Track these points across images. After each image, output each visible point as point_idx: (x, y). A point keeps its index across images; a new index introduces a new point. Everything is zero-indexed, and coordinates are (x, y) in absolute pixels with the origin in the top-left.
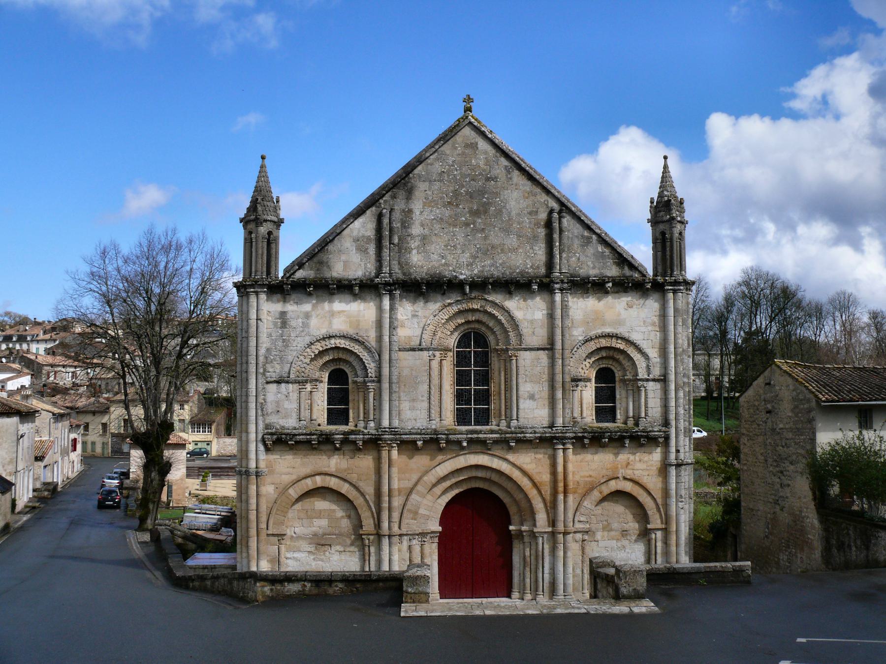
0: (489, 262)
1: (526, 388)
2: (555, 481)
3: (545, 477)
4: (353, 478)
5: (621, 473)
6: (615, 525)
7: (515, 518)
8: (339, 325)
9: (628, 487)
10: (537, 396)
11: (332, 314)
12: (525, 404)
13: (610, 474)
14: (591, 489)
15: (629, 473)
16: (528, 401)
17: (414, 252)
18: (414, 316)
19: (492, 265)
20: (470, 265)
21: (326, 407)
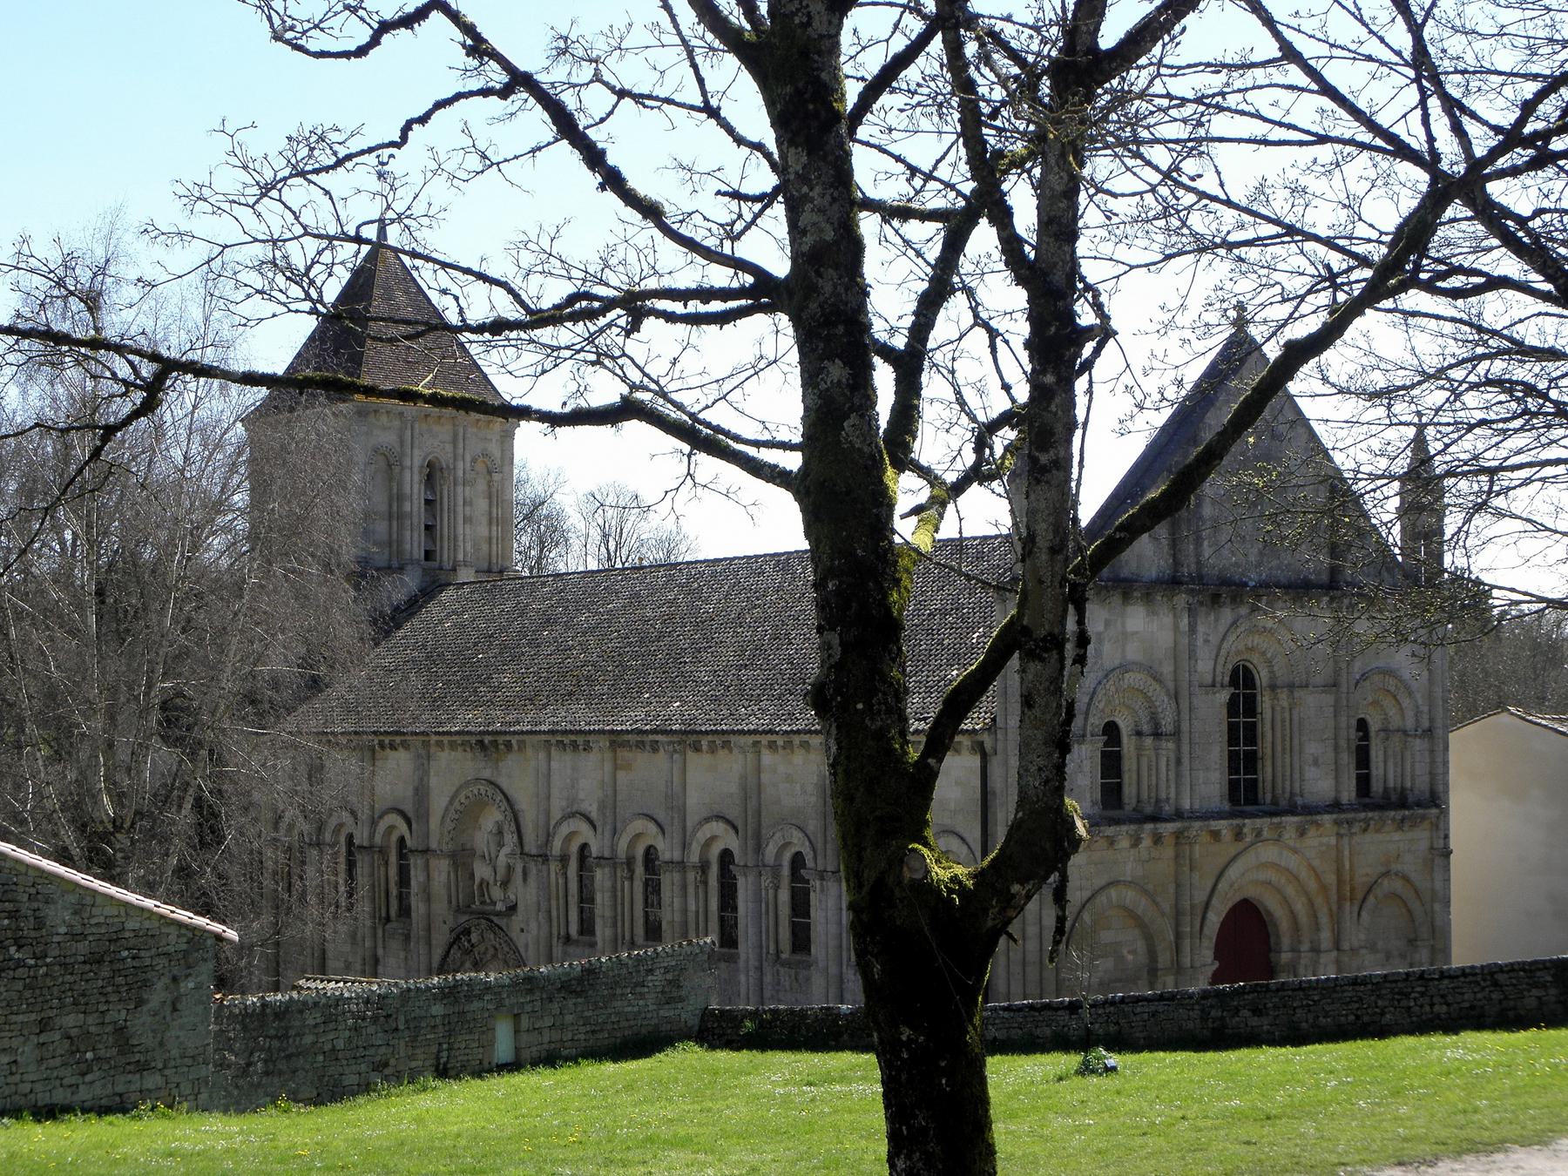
0: (1275, 563)
1: (1312, 748)
2: (1340, 882)
3: (1331, 879)
4: (1150, 887)
5: (1395, 867)
6: (1380, 944)
7: (1286, 942)
8: (1133, 652)
9: (1397, 885)
10: (1320, 761)
11: (1125, 636)
12: (1311, 773)
13: (1383, 870)
14: (1368, 892)
15: (1399, 867)
16: (1313, 769)
17: (1206, 543)
18: (1206, 641)
19: (1279, 567)
20: (1259, 564)
21: (1100, 781)
